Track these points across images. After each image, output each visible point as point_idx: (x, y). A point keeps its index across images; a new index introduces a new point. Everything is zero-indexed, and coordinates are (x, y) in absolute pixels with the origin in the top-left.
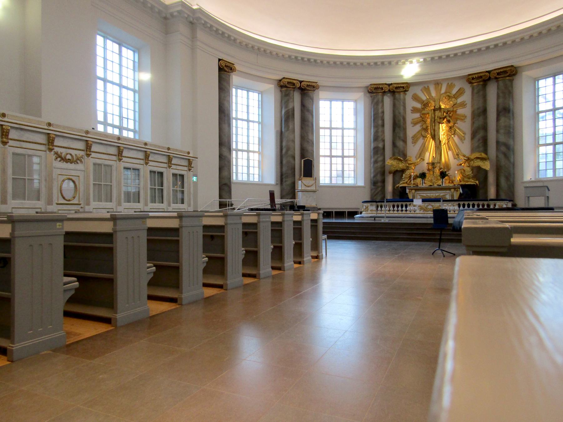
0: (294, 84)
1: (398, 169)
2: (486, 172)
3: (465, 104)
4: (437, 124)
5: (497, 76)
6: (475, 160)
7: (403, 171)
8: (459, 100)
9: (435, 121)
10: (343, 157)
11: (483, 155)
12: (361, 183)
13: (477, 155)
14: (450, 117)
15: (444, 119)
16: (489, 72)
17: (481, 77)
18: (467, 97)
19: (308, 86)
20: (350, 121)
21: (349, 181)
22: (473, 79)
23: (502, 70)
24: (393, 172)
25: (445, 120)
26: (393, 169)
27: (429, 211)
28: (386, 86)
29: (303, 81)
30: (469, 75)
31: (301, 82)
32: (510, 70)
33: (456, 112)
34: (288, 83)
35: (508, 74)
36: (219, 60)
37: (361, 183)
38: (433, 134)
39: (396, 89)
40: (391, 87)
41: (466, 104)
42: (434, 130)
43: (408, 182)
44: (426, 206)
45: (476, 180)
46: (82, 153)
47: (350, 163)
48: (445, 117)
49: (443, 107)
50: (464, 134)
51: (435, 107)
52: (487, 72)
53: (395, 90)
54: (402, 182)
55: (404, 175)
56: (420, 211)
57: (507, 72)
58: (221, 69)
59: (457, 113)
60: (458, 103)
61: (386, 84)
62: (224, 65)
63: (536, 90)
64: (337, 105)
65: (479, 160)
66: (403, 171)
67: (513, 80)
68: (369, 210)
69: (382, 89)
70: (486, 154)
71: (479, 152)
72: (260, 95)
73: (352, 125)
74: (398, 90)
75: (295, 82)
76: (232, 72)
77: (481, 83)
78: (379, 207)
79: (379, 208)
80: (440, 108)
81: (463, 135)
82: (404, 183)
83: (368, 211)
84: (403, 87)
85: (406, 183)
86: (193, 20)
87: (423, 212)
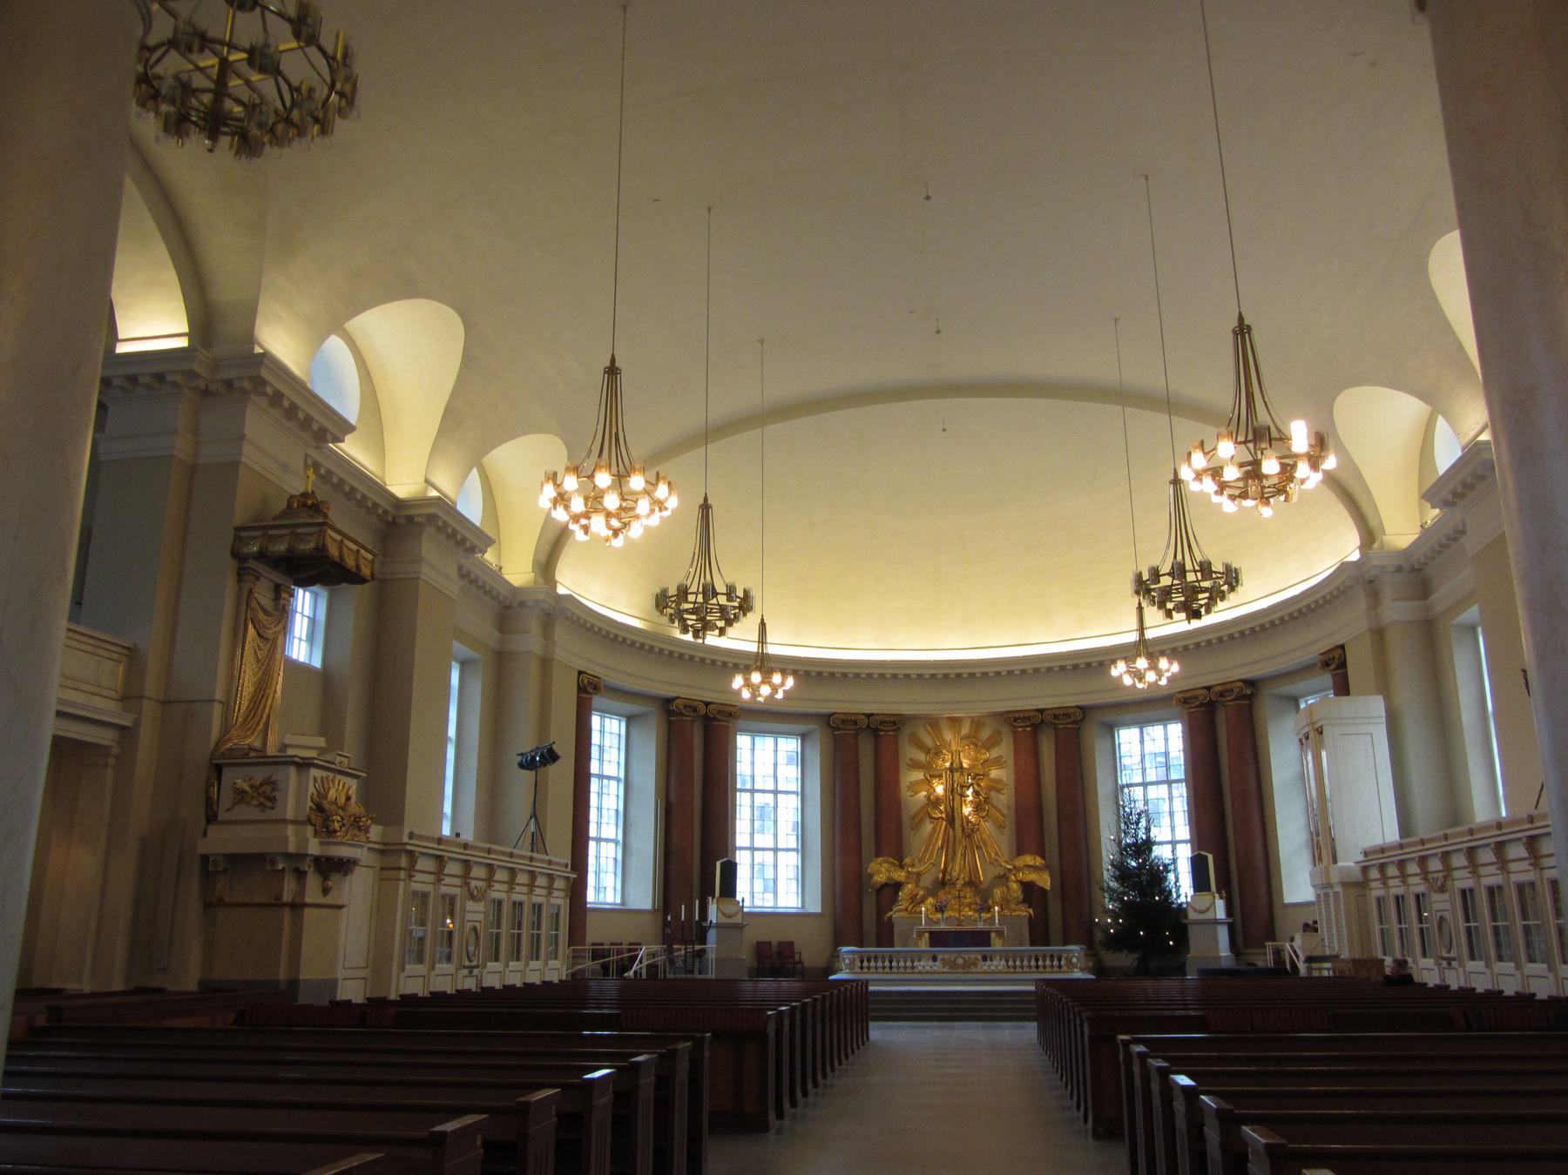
0: (695, 709)
1: (889, 882)
2: (1043, 890)
3: (1003, 760)
4: (957, 798)
5: (1055, 721)
6: (1026, 868)
7: (898, 886)
8: (995, 753)
9: (952, 791)
10: (776, 850)
11: (1039, 861)
12: (815, 907)
13: (1029, 859)
14: (979, 785)
15: (968, 788)
16: (1041, 711)
17: (1029, 718)
18: (1004, 750)
19: (719, 712)
20: (790, 776)
21: (788, 899)
22: (1016, 720)
23: (1061, 712)
24: (878, 887)
25: (971, 790)
26: (879, 879)
27: (958, 968)
28: (863, 717)
29: (711, 703)
30: (1008, 712)
31: (707, 704)
32: (1074, 712)
33: (989, 775)
34: (685, 706)
35: (1071, 720)
36: (580, 673)
37: (815, 907)
38: (950, 815)
39: (880, 724)
40: (872, 719)
41: (1005, 762)
42: (953, 809)
43: (909, 909)
44: (953, 959)
45: (1029, 907)
46: (483, 884)
47: (790, 861)
48: (972, 785)
49: (965, 765)
50: (1003, 816)
51: (952, 764)
52: (1038, 710)
53: (881, 727)
54: (897, 908)
55: (900, 894)
56: (944, 967)
57: (1070, 717)
58: (581, 689)
59: (991, 776)
60: (991, 758)
61: (863, 714)
62: (586, 682)
63: (1113, 750)
64: (765, 744)
65: (1032, 870)
66: (898, 886)
67: (1079, 729)
68: (856, 968)
69: (855, 723)
70: (1043, 857)
71: (1034, 854)
72: (623, 725)
73: (794, 786)
74: (885, 728)
75: (696, 704)
76: (596, 694)
77: (1028, 729)
78: (873, 961)
79: (865, 964)
80: (962, 767)
81: (1002, 819)
82: (901, 911)
83: (854, 968)
84: (894, 723)
85: (906, 910)
86: (554, 610)
87: (949, 971)
